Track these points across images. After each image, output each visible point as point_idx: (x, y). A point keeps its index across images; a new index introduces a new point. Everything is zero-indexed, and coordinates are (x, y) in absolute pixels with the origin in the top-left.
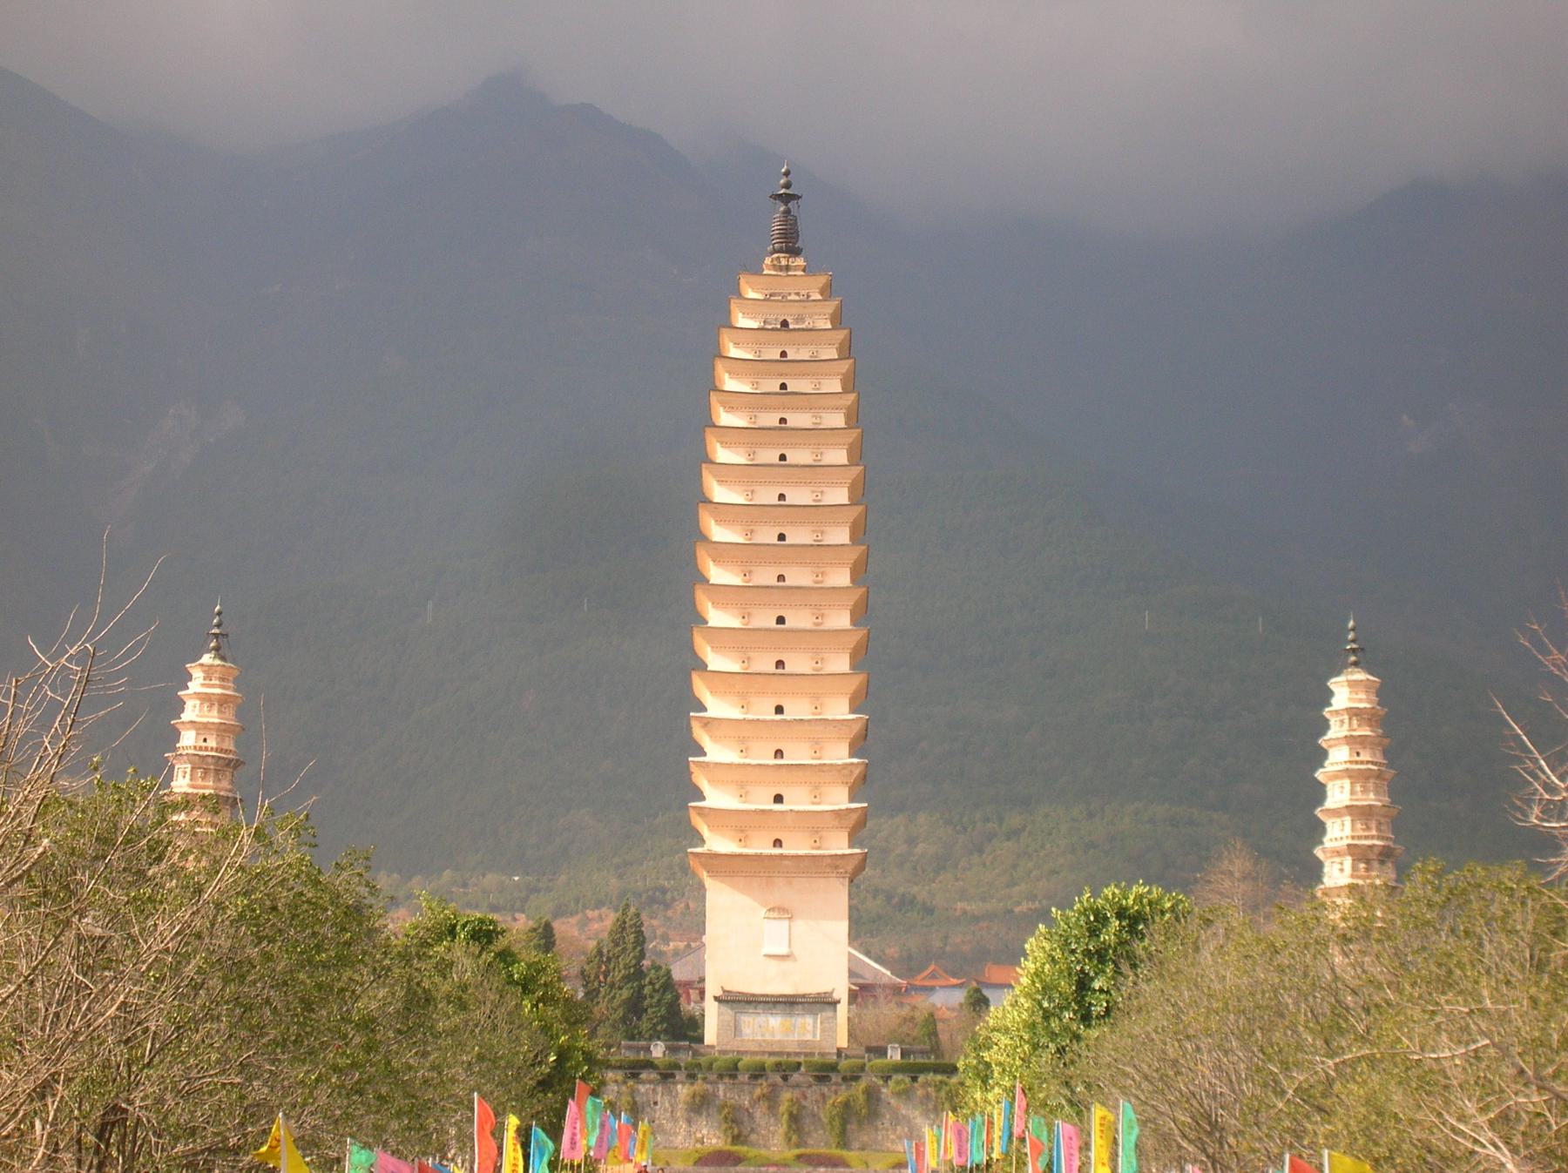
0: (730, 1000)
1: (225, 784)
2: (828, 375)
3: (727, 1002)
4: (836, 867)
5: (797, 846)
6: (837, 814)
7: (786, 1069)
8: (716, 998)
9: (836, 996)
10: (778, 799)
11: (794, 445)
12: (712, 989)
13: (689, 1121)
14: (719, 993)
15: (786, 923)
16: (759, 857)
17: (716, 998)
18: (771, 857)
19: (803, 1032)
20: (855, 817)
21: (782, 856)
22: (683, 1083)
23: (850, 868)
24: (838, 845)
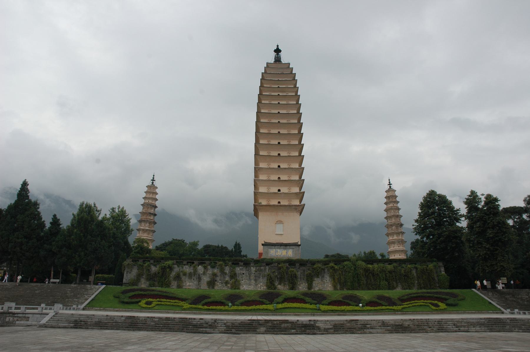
0: (265, 245)
1: (153, 211)
2: (291, 84)
3: (266, 245)
4: (296, 209)
5: (284, 202)
6: (296, 194)
7: (291, 262)
8: (263, 245)
9: (299, 243)
10: (279, 190)
11: (282, 100)
12: (261, 241)
13: (256, 280)
14: (263, 243)
15: (282, 225)
16: (274, 205)
17: (263, 245)
18: (277, 206)
19: (289, 254)
20: (301, 195)
21: (281, 205)
22: (253, 266)
23: (300, 209)
24: (296, 202)
